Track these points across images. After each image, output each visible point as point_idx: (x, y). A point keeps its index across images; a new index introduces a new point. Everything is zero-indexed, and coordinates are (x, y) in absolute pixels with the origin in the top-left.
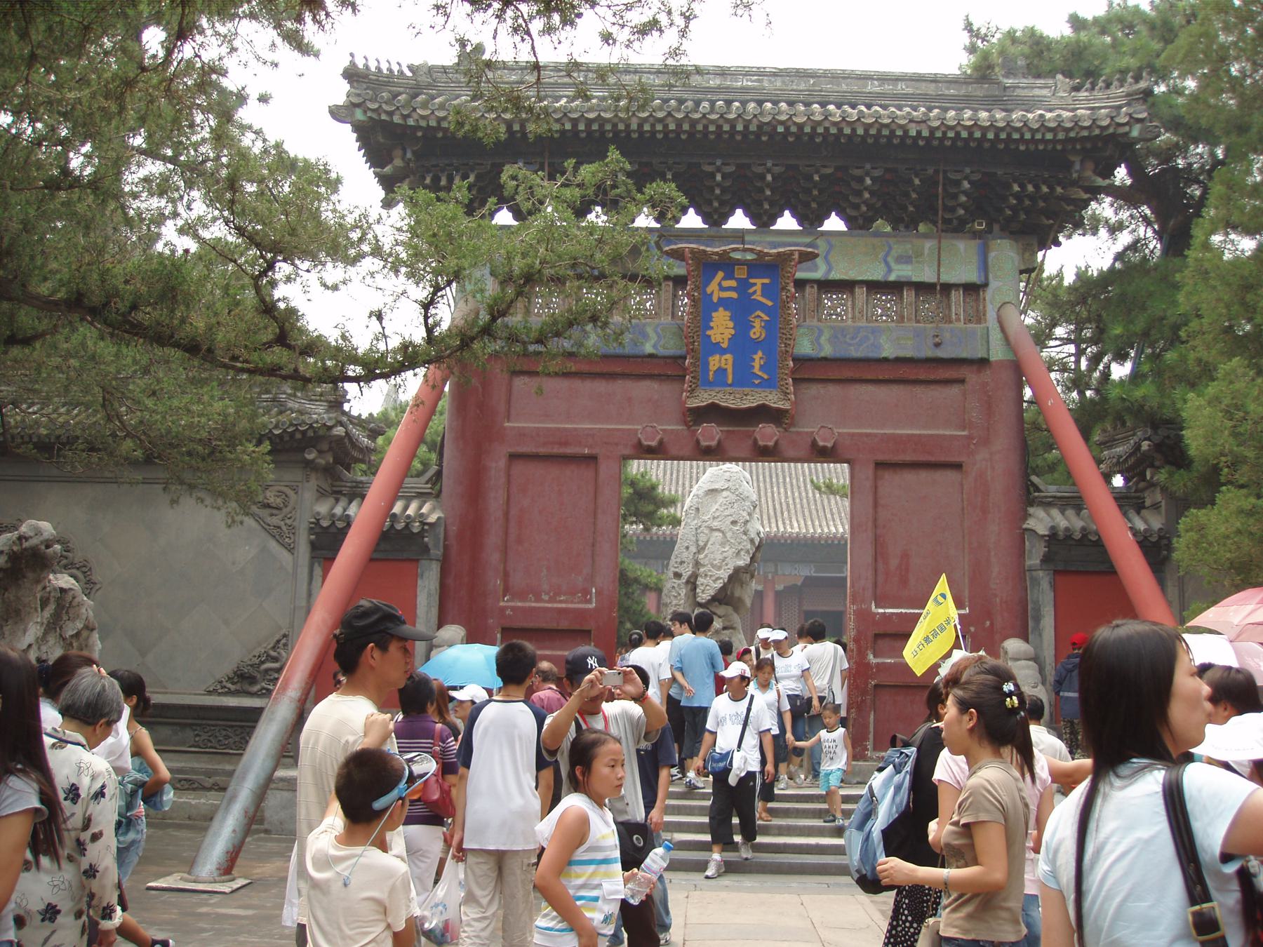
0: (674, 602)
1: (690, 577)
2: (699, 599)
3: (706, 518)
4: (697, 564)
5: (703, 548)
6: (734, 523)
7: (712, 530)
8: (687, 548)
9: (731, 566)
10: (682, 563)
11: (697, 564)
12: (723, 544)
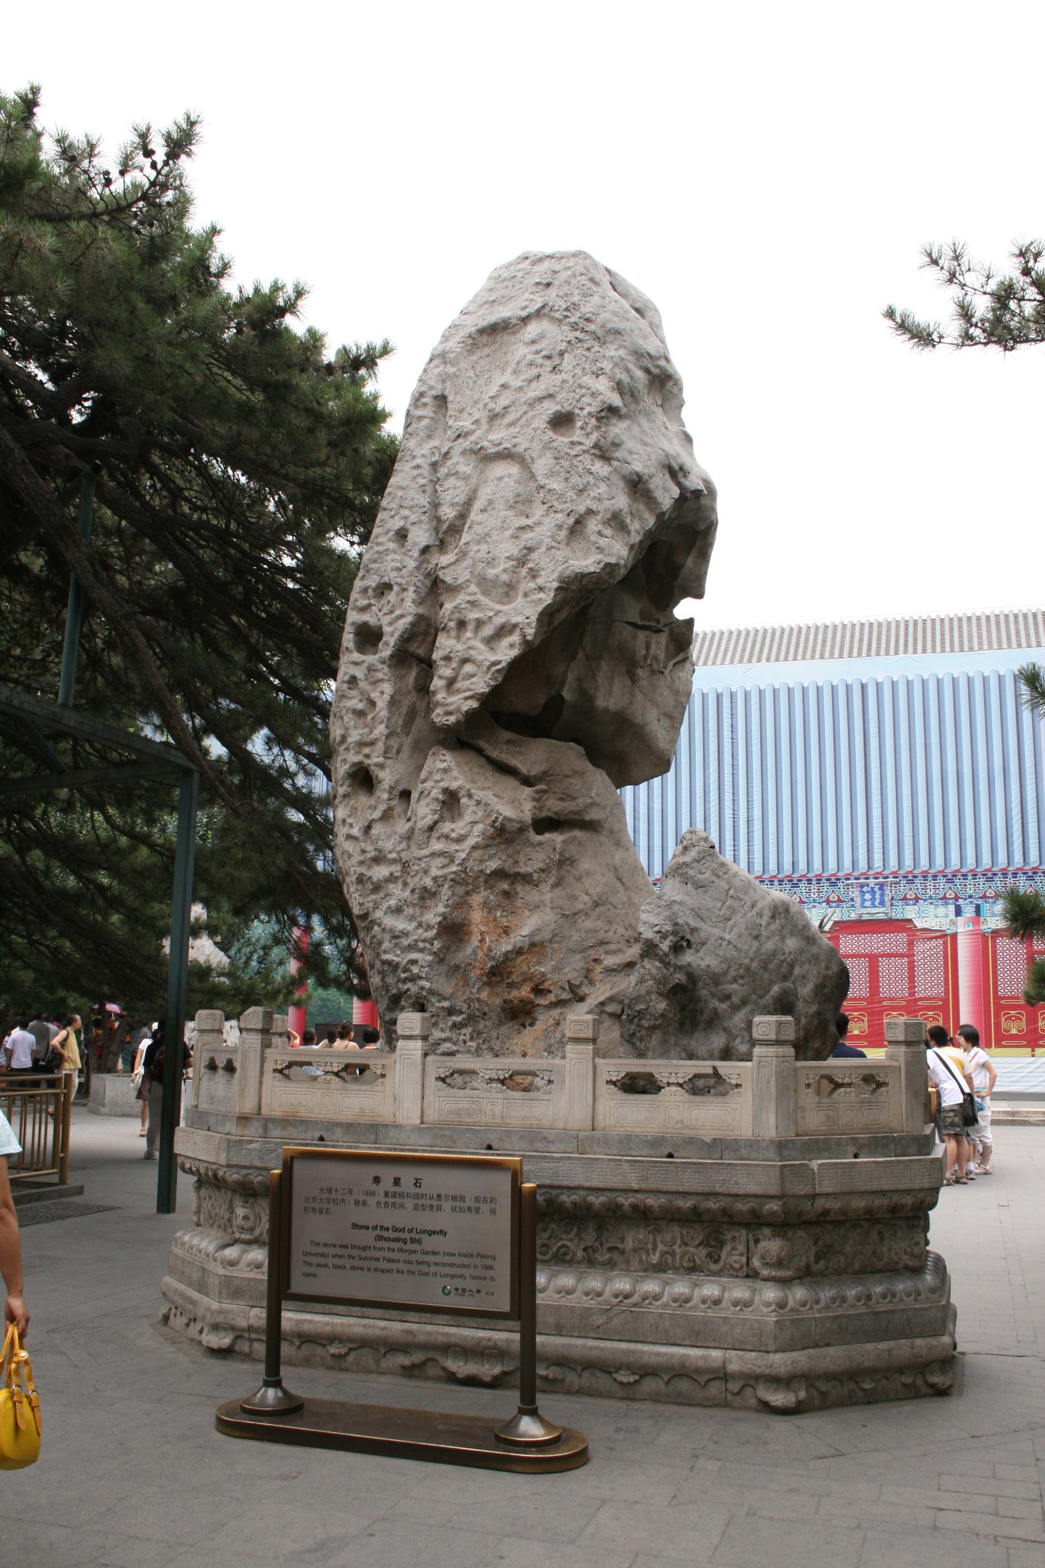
0: (354, 737)
1: (409, 637)
2: (438, 717)
3: (466, 424)
4: (435, 587)
5: (455, 529)
6: (562, 421)
7: (485, 457)
8: (402, 535)
9: (550, 579)
10: (384, 588)
11: (435, 587)
12: (521, 503)
